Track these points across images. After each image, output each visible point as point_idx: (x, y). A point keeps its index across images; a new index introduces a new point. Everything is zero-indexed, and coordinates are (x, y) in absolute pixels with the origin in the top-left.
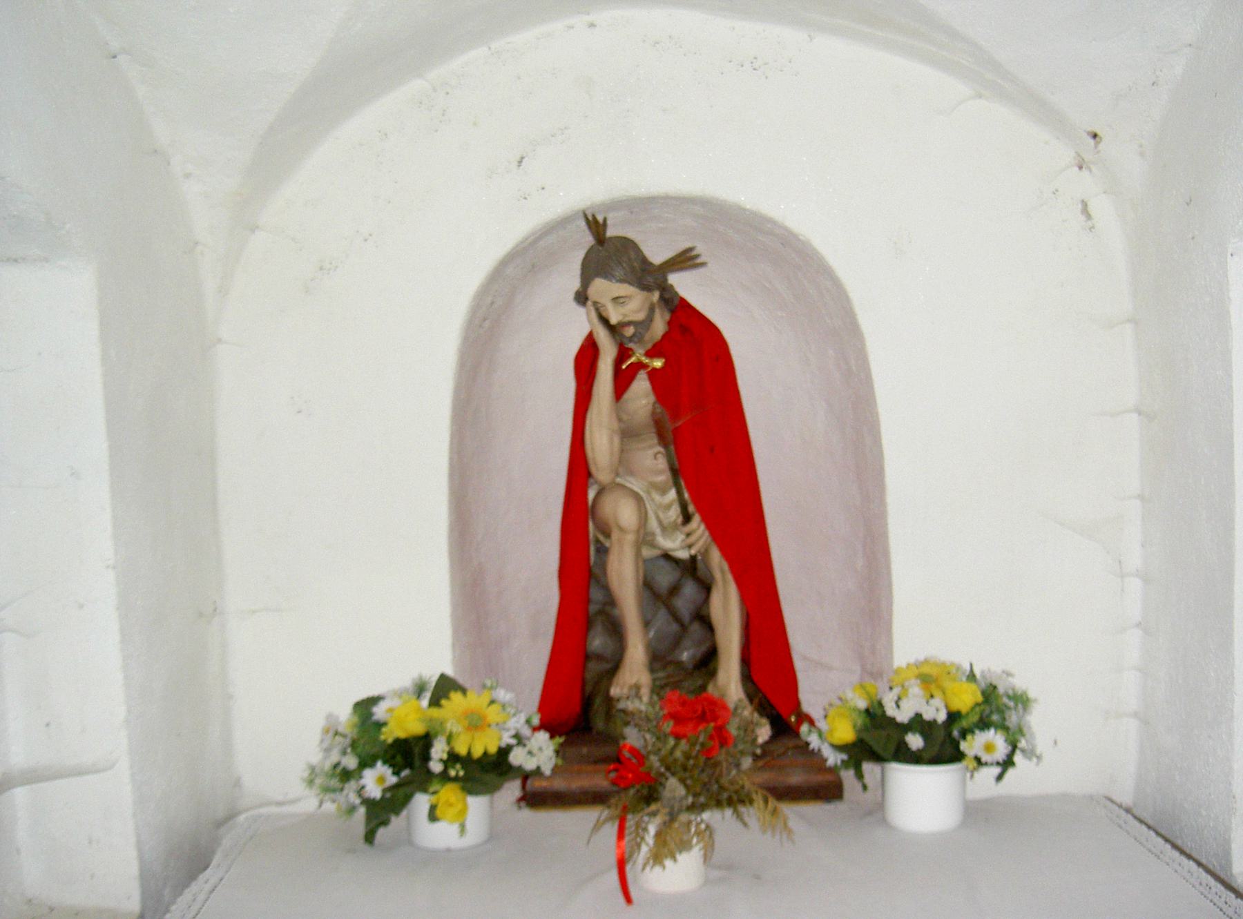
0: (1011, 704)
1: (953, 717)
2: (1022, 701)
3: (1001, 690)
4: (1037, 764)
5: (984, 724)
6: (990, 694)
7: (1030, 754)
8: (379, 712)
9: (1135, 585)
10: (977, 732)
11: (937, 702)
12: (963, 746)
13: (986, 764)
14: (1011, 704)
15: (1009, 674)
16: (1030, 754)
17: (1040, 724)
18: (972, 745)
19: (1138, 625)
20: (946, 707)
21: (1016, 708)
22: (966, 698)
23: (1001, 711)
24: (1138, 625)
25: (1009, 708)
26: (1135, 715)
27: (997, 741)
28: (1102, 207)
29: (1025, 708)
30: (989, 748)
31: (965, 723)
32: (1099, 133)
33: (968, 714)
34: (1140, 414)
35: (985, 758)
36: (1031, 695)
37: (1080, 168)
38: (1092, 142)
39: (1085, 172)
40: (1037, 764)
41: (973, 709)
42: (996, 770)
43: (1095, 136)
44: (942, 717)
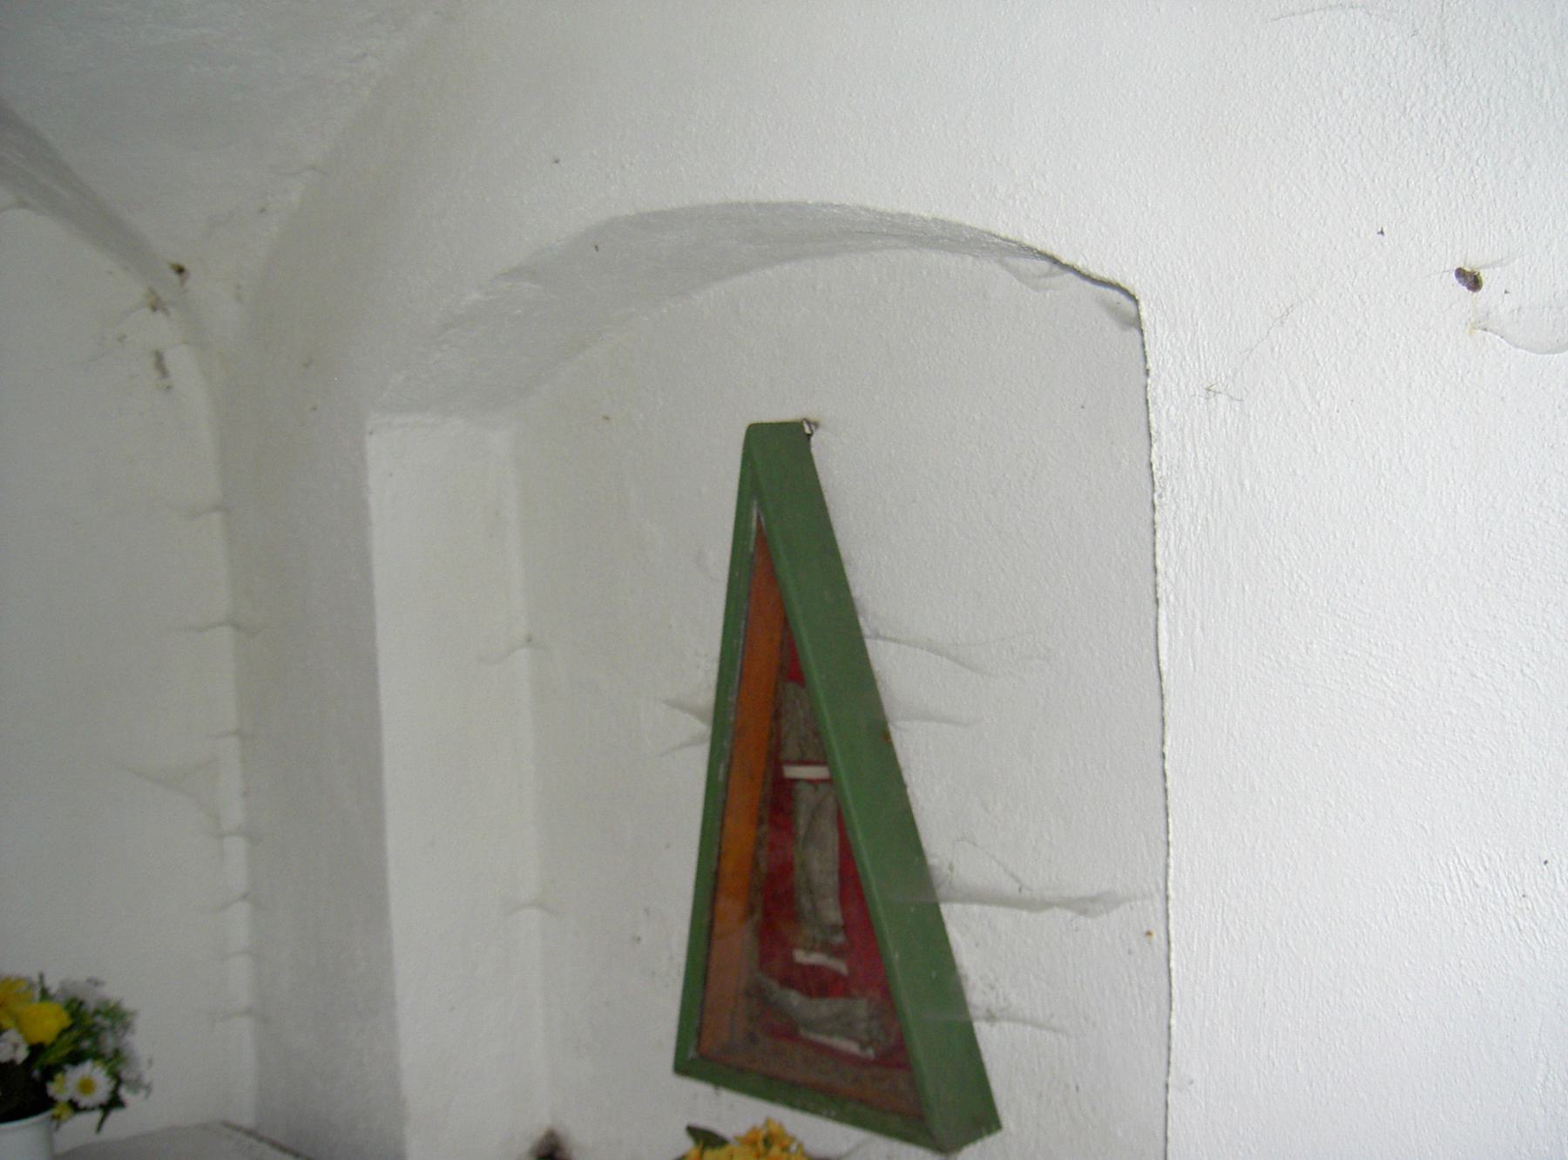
0: (107, 1023)
1: (36, 1050)
2: (117, 1016)
3: (91, 1005)
4: (147, 1096)
5: (76, 1058)
6: (75, 1008)
7: (137, 1085)
8: (142, 1093)
9: (237, 847)
10: (68, 1067)
11: (12, 1036)
12: (53, 1089)
13: (85, 1109)
14: (107, 1023)
15: (97, 983)
16: (137, 1085)
17: (141, 1042)
18: (64, 1087)
19: (245, 897)
20: (26, 1038)
21: (112, 1028)
22: (49, 1023)
23: (92, 1032)
24: (245, 897)
25: (103, 1029)
26: (249, 1011)
27: (93, 1072)
28: (181, 360)
29: (127, 1027)
30: (87, 1086)
31: (51, 1059)
32: (186, 266)
33: (53, 1045)
34: (237, 627)
35: (84, 1101)
36: (128, 1005)
37: (154, 309)
38: (175, 277)
39: (160, 315)
40: (147, 1096)
41: (60, 1036)
42: (96, 1116)
43: (180, 270)
44: (22, 1054)
